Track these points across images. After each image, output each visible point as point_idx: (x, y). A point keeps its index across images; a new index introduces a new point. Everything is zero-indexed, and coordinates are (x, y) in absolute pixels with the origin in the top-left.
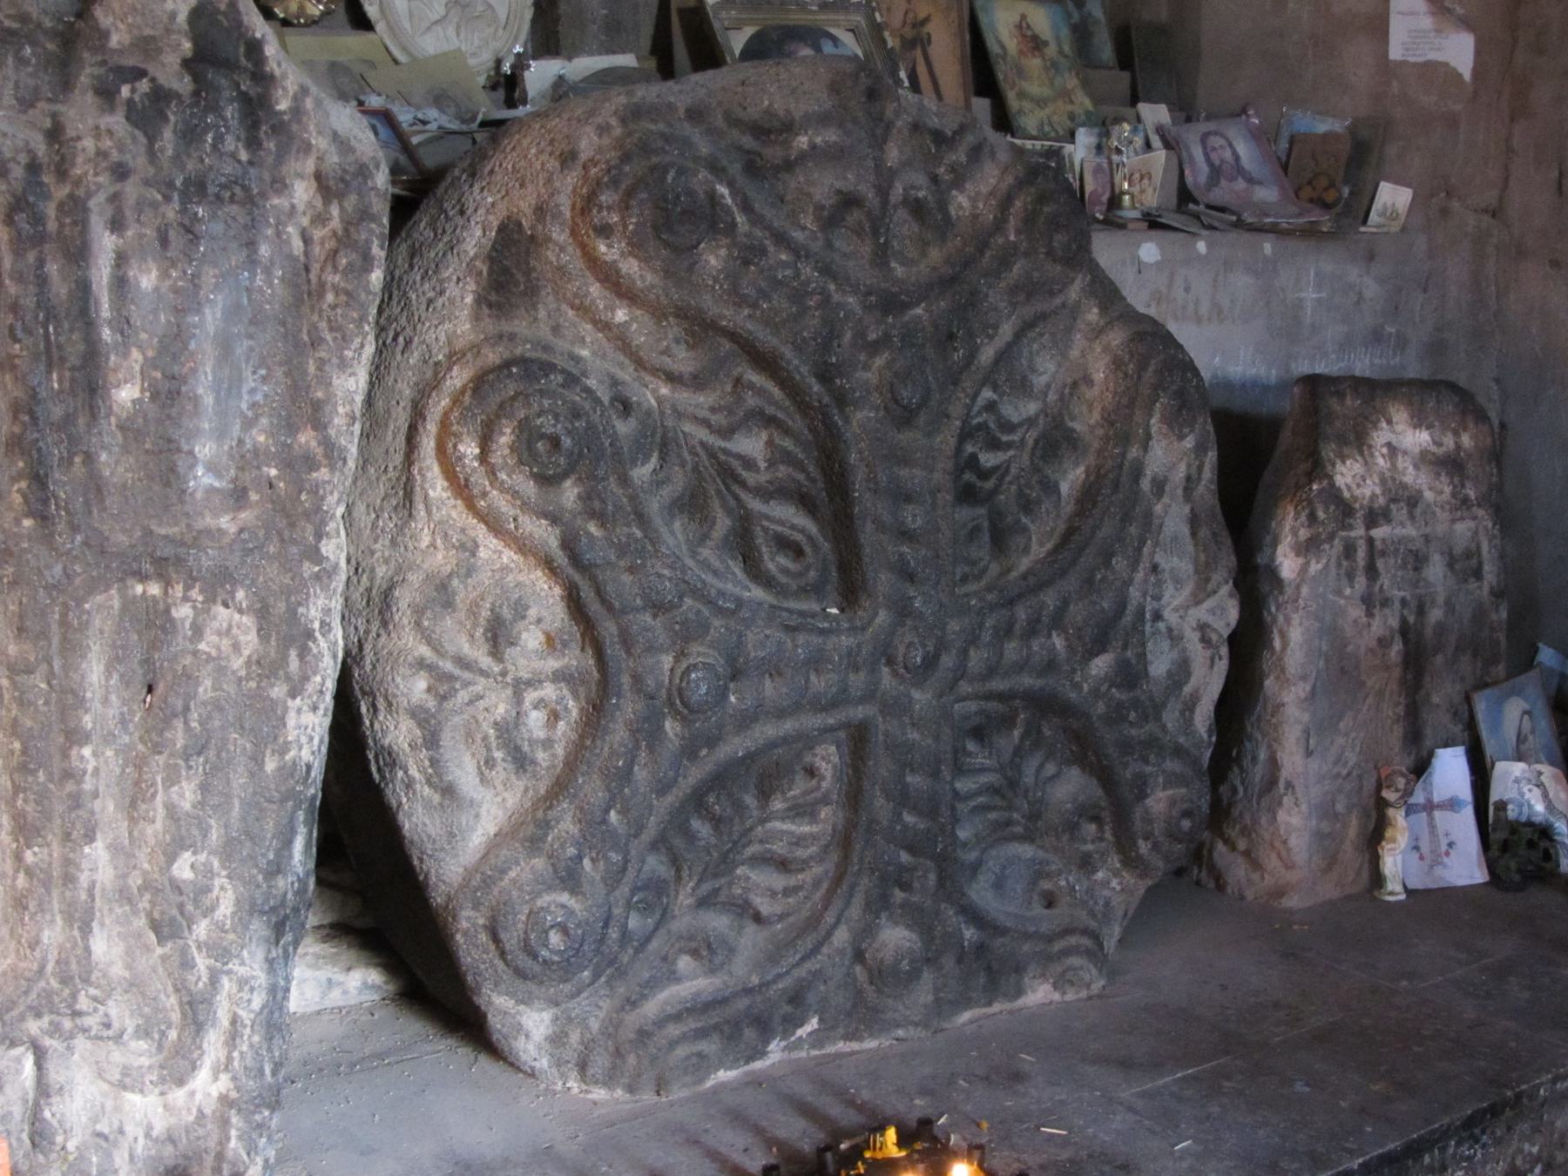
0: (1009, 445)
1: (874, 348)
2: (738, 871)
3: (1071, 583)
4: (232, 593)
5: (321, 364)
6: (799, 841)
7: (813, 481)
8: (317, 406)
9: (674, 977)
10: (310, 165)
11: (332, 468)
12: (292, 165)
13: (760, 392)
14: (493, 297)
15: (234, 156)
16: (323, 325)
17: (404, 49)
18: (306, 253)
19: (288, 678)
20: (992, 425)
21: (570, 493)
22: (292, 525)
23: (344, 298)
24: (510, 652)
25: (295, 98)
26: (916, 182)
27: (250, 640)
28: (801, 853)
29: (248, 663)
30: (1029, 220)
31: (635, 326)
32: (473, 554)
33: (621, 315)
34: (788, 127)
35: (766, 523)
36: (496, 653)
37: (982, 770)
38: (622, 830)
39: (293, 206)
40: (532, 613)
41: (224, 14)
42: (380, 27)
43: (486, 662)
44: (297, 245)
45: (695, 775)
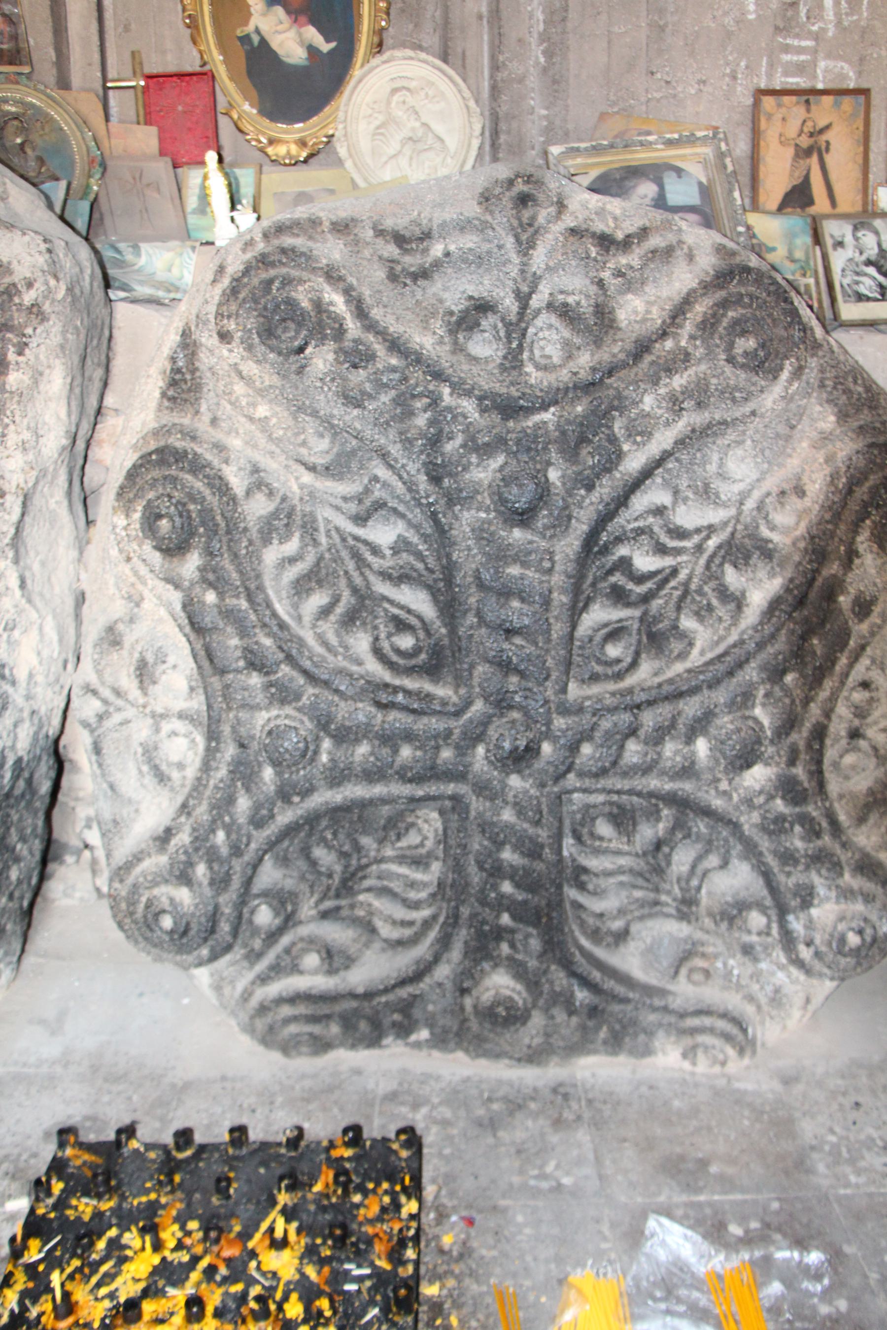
0: (678, 551)
1: (485, 451)
3: (720, 696)
6: (412, 885)
7: (432, 571)
9: (295, 969)
13: (385, 485)
17: (365, 180)
20: (656, 529)
24: (152, 689)
26: (575, 285)
30: (708, 326)
31: (274, 420)
32: (138, 605)
33: (262, 411)
35: (386, 605)
36: (142, 687)
37: (618, 853)
40: (171, 660)
42: (349, 164)
43: (135, 693)
45: (285, 817)
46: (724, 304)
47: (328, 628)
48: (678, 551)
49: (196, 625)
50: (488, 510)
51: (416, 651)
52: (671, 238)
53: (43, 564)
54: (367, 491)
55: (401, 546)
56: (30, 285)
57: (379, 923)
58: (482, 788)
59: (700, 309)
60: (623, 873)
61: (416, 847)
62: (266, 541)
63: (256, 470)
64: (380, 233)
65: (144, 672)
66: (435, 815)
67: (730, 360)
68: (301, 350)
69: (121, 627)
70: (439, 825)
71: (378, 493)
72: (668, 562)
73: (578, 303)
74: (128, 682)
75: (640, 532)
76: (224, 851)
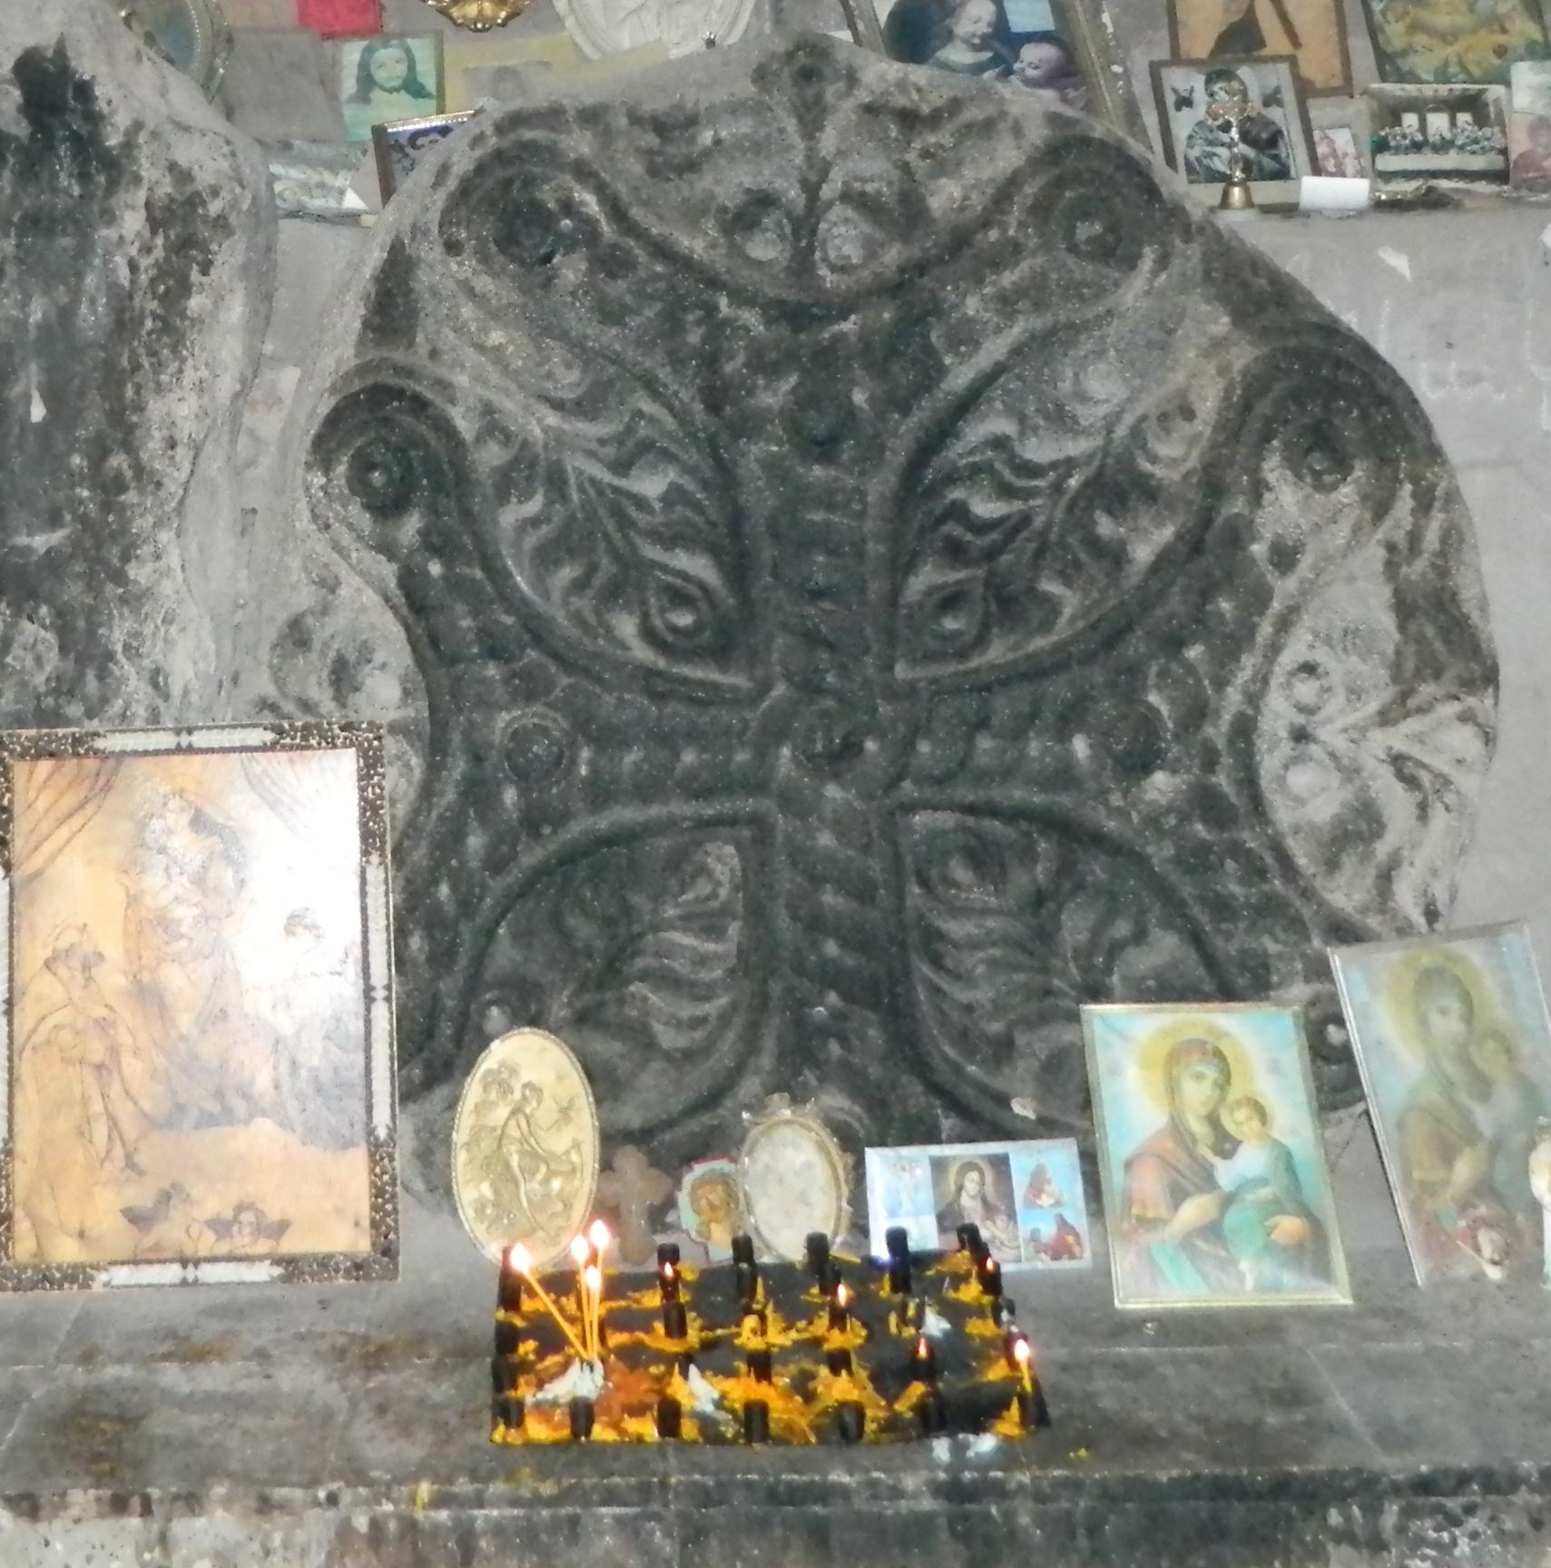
0: (1028, 494)
2: (632, 988)
4: (37, 608)
5: (138, 389)
6: (702, 961)
7: (713, 524)
8: (131, 429)
10: (142, 195)
11: (141, 491)
12: (122, 197)
13: (652, 420)
14: (377, 320)
15: (67, 192)
16: (142, 350)
17: (595, 45)
18: (132, 282)
19: (84, 698)
20: (998, 465)
21: (410, 527)
22: (98, 547)
23: (159, 324)
25: (127, 133)
26: (872, 168)
27: (52, 659)
28: (704, 976)
29: (48, 680)
30: (1040, 211)
31: (511, 348)
33: (496, 337)
34: (692, 122)
35: (658, 573)
36: (340, 699)
37: (985, 911)
38: (450, 909)
39: (121, 237)
40: (379, 657)
41: (50, 60)
42: (570, 22)
44: (124, 275)
46: (1058, 184)
47: (584, 604)
48: (1028, 494)
49: (415, 602)
50: (779, 443)
51: (698, 628)
52: (991, 110)
53: (201, 550)
54: (630, 429)
55: (674, 496)
56: (215, 192)
57: (658, 1028)
58: (790, 801)
59: (1031, 189)
60: (994, 944)
61: (708, 898)
62: (502, 496)
63: (488, 409)
64: (635, 119)
65: (343, 677)
66: (730, 849)
67: (1073, 248)
68: (548, 258)
69: (310, 620)
70: (736, 862)
71: (643, 430)
72: (1018, 505)
73: (879, 192)
74: (321, 694)
75: (976, 469)
76: (450, 909)
